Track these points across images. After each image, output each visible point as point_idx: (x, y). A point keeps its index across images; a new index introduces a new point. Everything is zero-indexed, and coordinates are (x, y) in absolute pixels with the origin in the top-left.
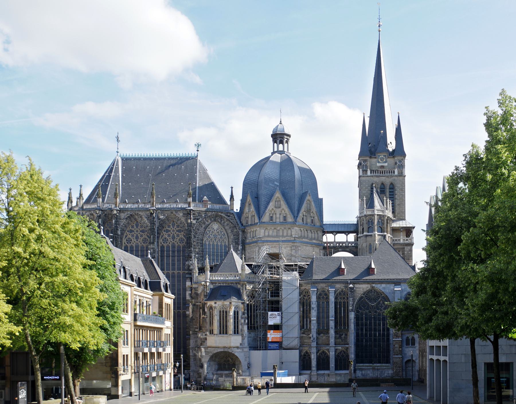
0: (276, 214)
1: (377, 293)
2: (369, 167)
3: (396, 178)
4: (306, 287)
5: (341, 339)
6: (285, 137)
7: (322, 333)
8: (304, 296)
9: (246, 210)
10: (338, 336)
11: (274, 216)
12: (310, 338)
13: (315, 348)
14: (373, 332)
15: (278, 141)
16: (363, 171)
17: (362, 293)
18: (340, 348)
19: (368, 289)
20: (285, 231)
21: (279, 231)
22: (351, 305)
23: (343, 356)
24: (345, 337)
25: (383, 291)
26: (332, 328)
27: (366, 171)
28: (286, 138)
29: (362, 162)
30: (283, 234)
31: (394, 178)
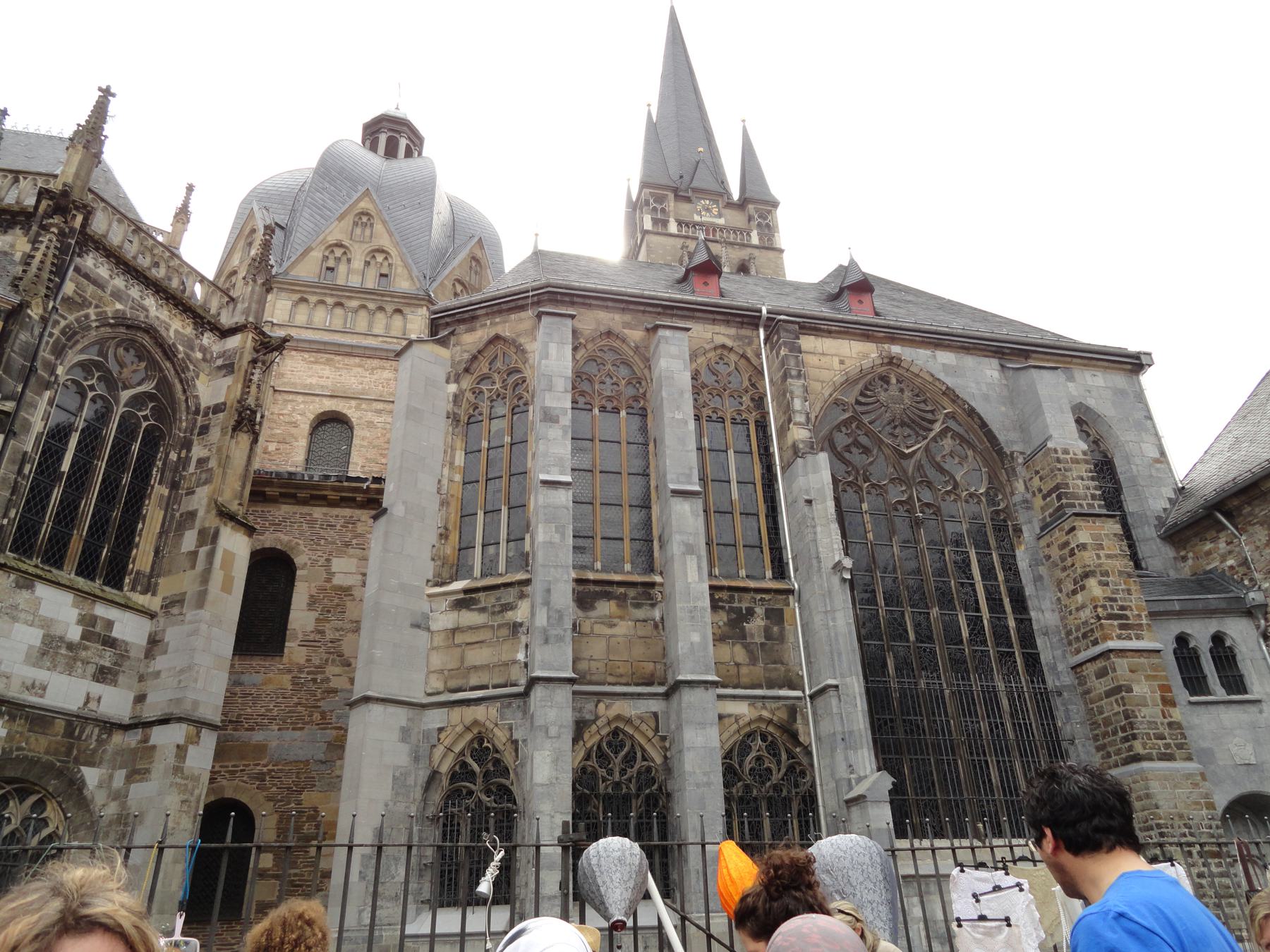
0: (349, 261)
1: (919, 393)
2: (671, 214)
3: (756, 252)
4: (492, 332)
5: (746, 646)
6: (405, 128)
7: (608, 596)
8: (484, 378)
9: (236, 261)
10: (723, 617)
11: (342, 268)
12: (515, 627)
13: (563, 695)
14: (935, 612)
15: (383, 138)
16: (655, 222)
17: (839, 379)
18: (742, 709)
19: (867, 364)
20: (380, 316)
21: (356, 311)
22: (800, 418)
23: (762, 774)
24: (767, 630)
25: (950, 381)
26: (690, 549)
27: (665, 223)
28: (409, 139)
29: (651, 201)
30: (370, 325)
31: (749, 250)
